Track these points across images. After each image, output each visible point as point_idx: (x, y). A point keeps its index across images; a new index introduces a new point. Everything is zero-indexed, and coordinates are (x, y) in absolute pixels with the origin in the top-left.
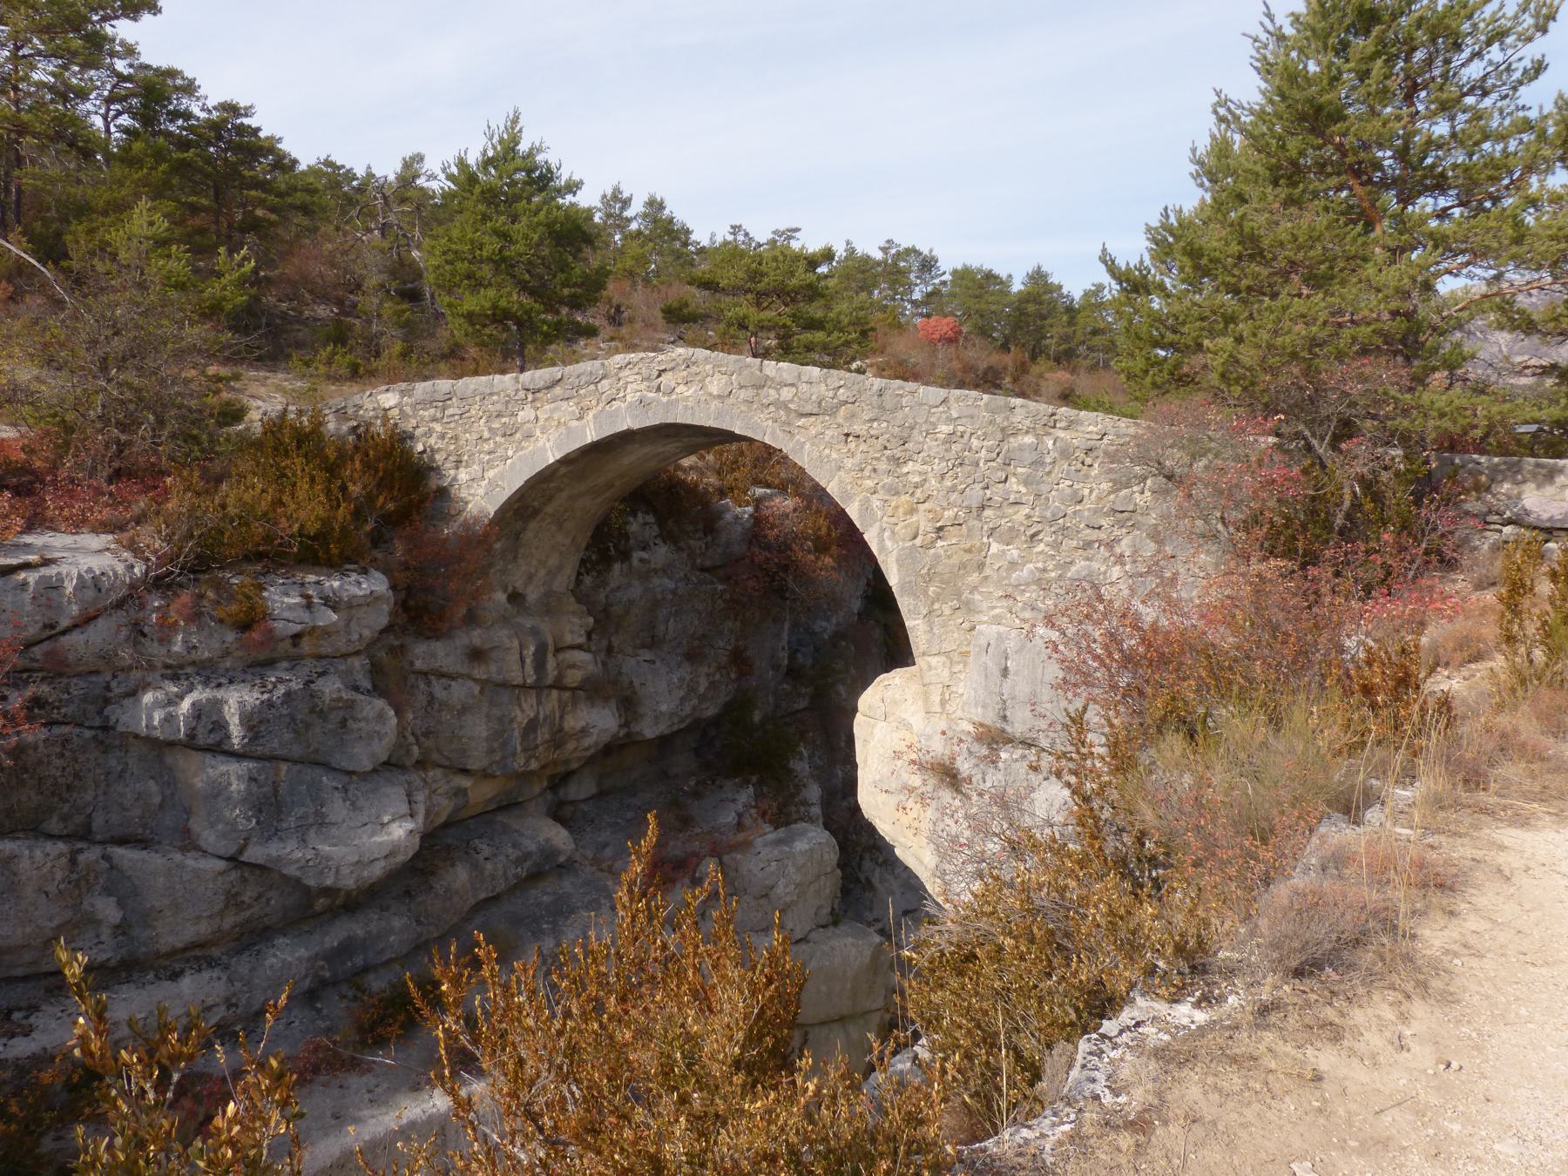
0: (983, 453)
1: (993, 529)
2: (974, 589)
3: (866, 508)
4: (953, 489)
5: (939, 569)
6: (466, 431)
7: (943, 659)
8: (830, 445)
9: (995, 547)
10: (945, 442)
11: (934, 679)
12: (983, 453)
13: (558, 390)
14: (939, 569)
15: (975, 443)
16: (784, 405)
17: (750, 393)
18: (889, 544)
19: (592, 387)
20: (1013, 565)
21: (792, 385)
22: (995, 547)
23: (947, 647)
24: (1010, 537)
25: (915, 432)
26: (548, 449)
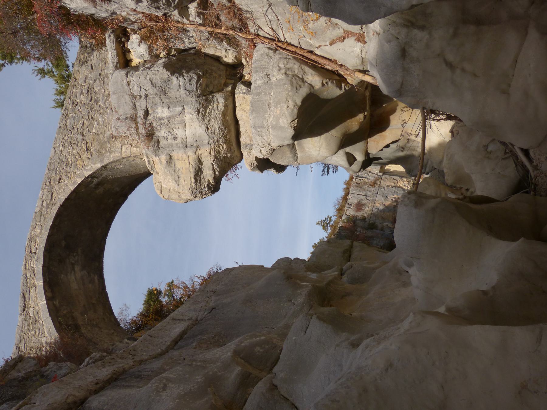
0: (69, 135)
1: (89, 131)
2: (104, 137)
3: (79, 176)
4: (77, 145)
5: (97, 149)
6: (30, 342)
7: (123, 147)
8: (60, 188)
9: (94, 131)
10: (64, 148)
11: (129, 150)
12: (69, 135)
13: (27, 296)
14: (97, 149)
15: (66, 138)
16: (48, 205)
17: (42, 217)
18: (89, 167)
19: (28, 280)
20: (98, 124)
21: (43, 202)
22: (94, 131)
23: (119, 146)
24: (91, 125)
25: (61, 158)
26: (43, 302)
